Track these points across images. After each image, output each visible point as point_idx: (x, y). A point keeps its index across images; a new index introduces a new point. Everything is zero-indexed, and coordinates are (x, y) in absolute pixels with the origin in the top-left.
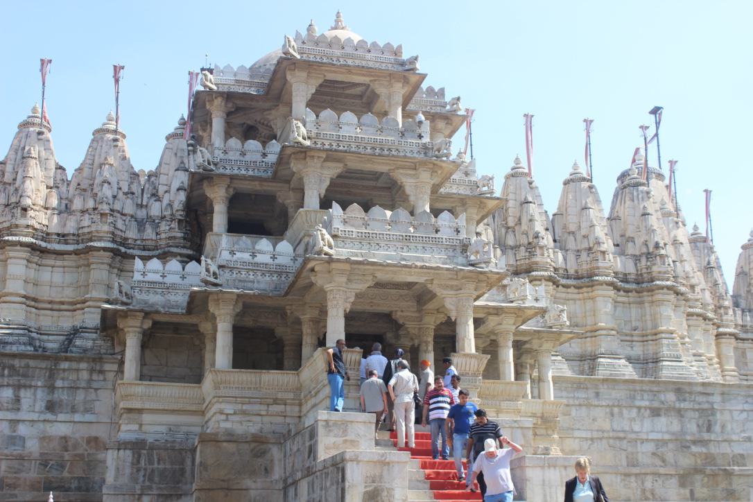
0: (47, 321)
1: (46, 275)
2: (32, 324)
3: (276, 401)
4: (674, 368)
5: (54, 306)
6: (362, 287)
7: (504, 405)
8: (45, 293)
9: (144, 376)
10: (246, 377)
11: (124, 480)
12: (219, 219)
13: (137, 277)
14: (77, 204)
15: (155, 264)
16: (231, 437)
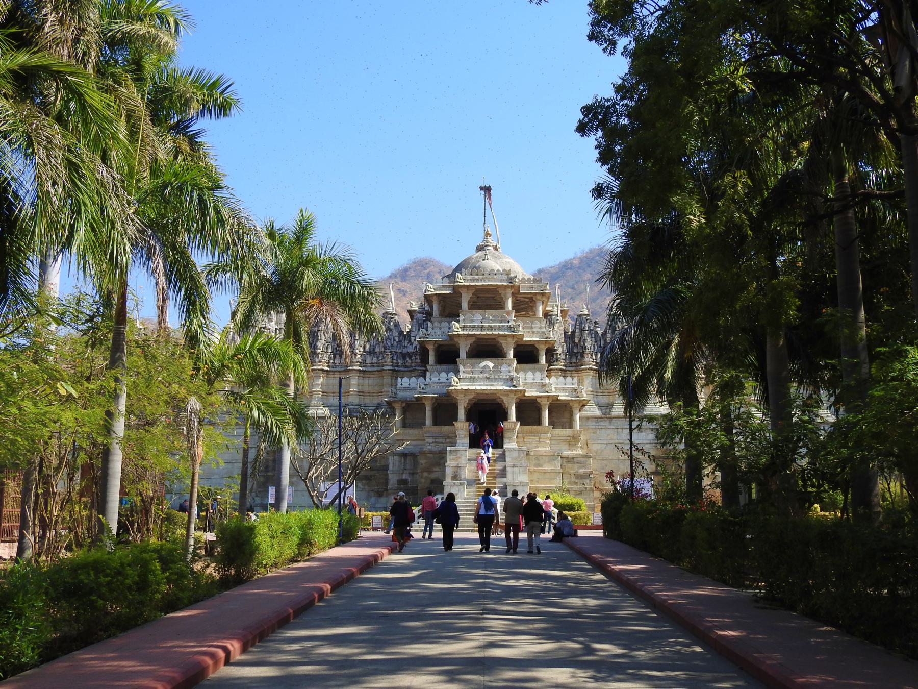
0: (367, 400)
1: (367, 381)
2: (362, 403)
3: (449, 438)
4: (652, 409)
5: (370, 394)
6: (471, 397)
7: (542, 436)
8: (366, 389)
9: (404, 425)
10: (436, 429)
11: (396, 468)
12: (432, 359)
13: (399, 385)
14: (377, 350)
15: (406, 380)
16: (431, 452)
